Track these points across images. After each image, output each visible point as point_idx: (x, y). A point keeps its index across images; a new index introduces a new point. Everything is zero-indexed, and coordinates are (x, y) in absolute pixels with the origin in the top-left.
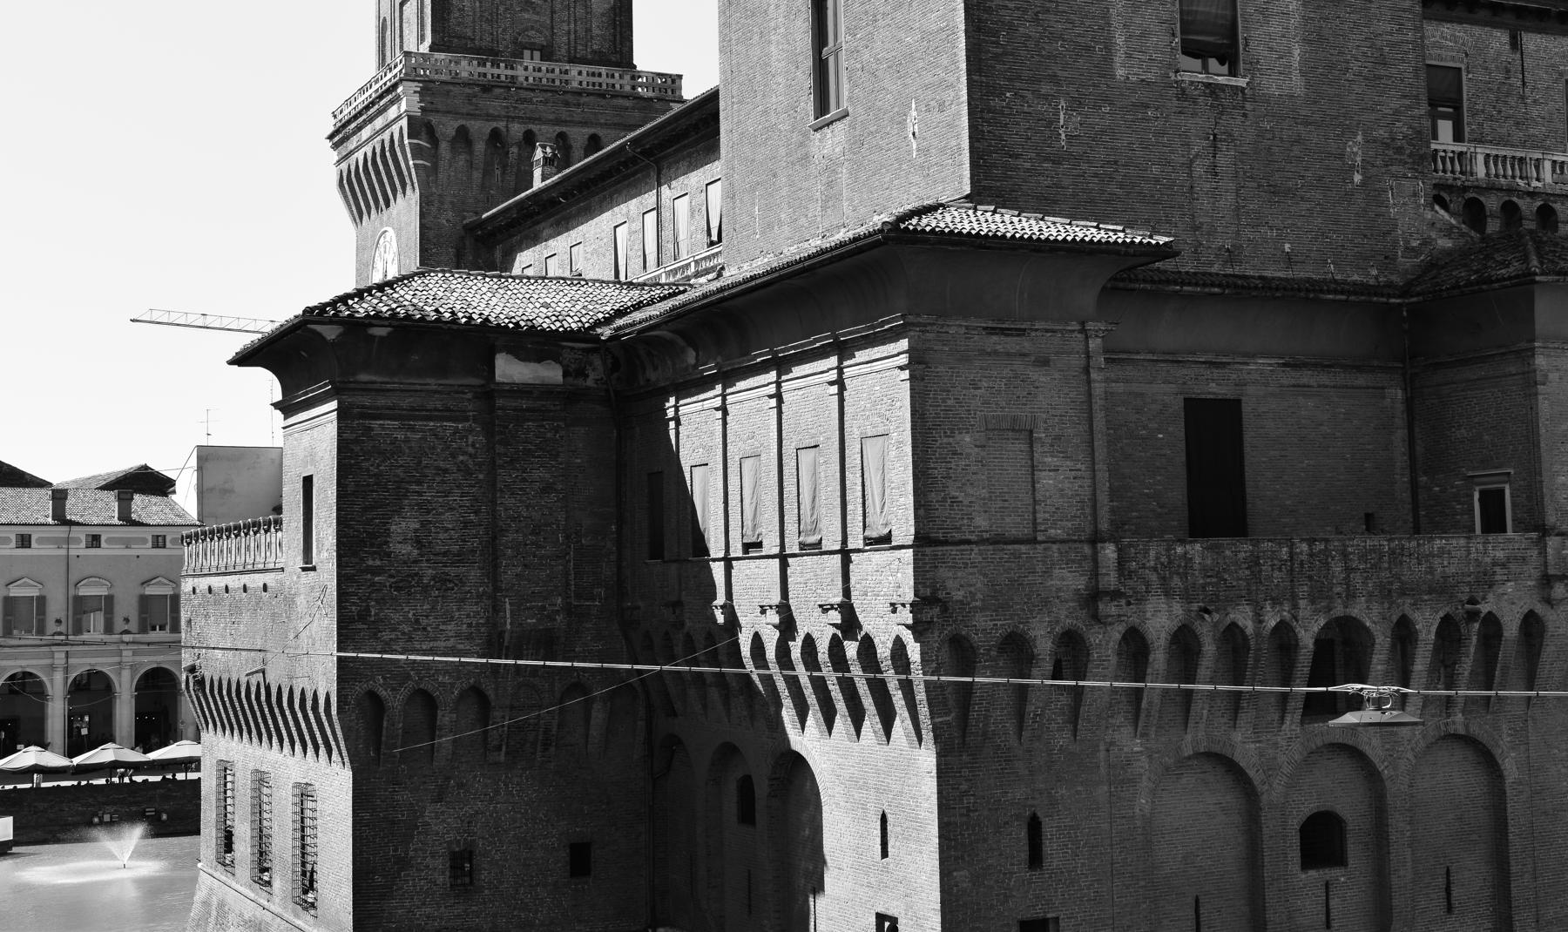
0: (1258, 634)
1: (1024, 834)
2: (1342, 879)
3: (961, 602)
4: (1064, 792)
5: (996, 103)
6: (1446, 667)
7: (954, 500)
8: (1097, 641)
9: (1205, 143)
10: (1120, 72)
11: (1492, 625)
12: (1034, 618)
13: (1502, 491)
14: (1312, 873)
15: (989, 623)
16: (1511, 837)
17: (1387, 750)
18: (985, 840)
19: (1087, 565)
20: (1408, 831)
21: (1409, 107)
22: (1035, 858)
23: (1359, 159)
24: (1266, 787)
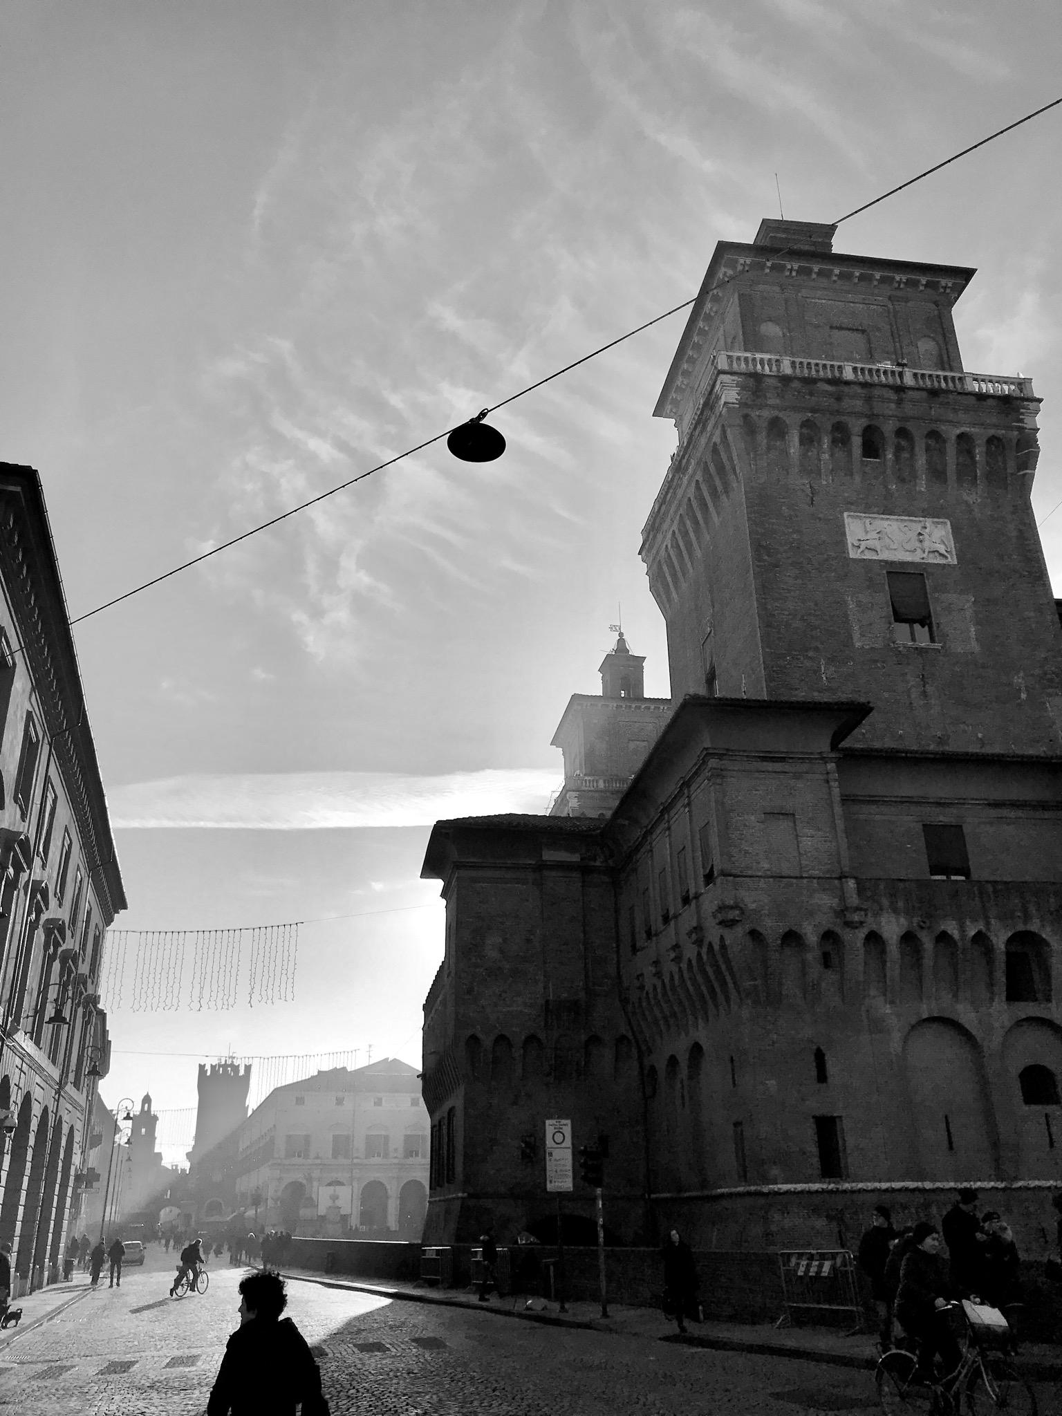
5: (781, 662)
7: (747, 852)
9: (918, 679)
10: (858, 644)
14: (1034, 1107)
21: (1054, 657)
22: (822, 1077)
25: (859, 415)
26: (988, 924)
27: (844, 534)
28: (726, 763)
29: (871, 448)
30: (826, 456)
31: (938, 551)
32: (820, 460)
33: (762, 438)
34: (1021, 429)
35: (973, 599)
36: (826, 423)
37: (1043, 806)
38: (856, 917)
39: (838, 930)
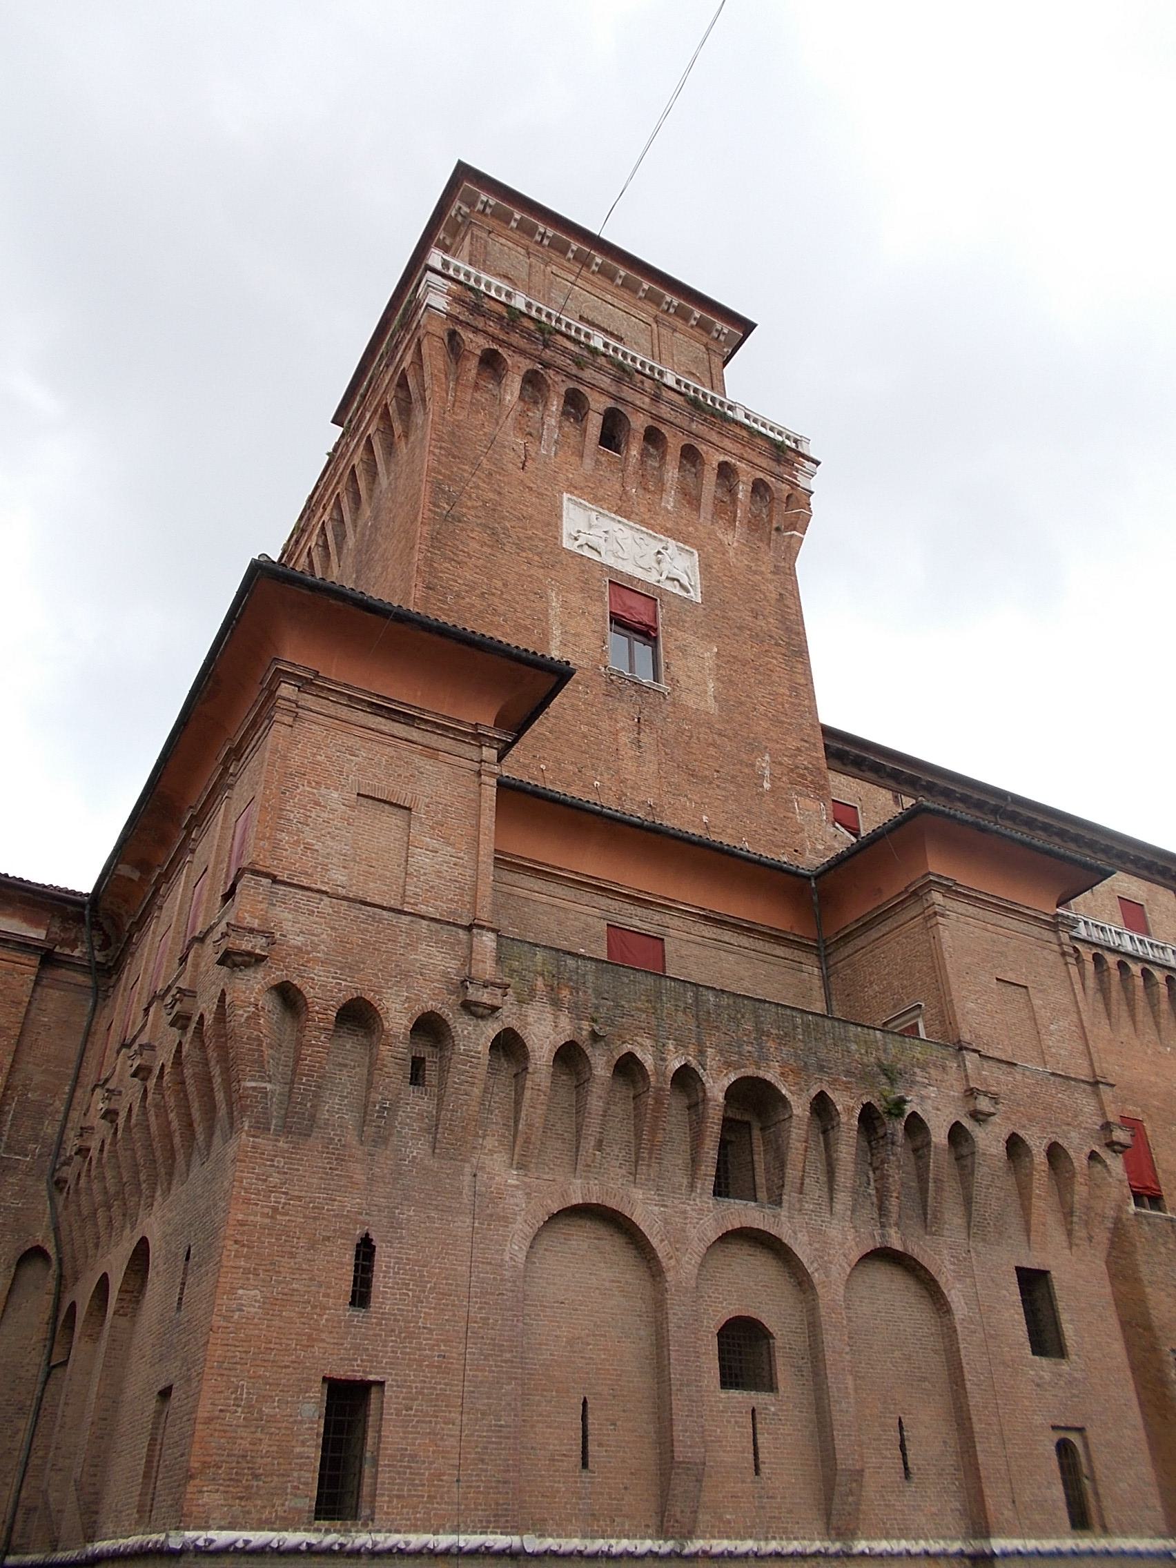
0: (657, 1072)
1: (349, 1257)
2: (773, 1409)
3: (300, 949)
4: (412, 1213)
6: (874, 1170)
8: (466, 1032)
9: (630, 722)
11: (916, 1125)
12: (389, 988)
13: (916, 1025)
15: (331, 980)
16: (968, 1385)
17: (816, 1250)
18: (292, 1256)
19: (462, 951)
20: (847, 1353)
22: (361, 1296)
23: (767, 773)
24: (673, 1262)
25: (603, 392)
26: (702, 1052)
27: (560, 517)
28: (308, 700)
29: (612, 435)
30: (553, 422)
31: (678, 581)
32: (543, 424)
33: (472, 365)
34: (794, 485)
35: (716, 650)
36: (559, 386)
37: (777, 938)
38: (485, 997)
39: (448, 1014)
